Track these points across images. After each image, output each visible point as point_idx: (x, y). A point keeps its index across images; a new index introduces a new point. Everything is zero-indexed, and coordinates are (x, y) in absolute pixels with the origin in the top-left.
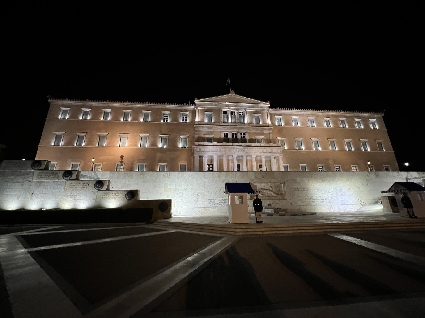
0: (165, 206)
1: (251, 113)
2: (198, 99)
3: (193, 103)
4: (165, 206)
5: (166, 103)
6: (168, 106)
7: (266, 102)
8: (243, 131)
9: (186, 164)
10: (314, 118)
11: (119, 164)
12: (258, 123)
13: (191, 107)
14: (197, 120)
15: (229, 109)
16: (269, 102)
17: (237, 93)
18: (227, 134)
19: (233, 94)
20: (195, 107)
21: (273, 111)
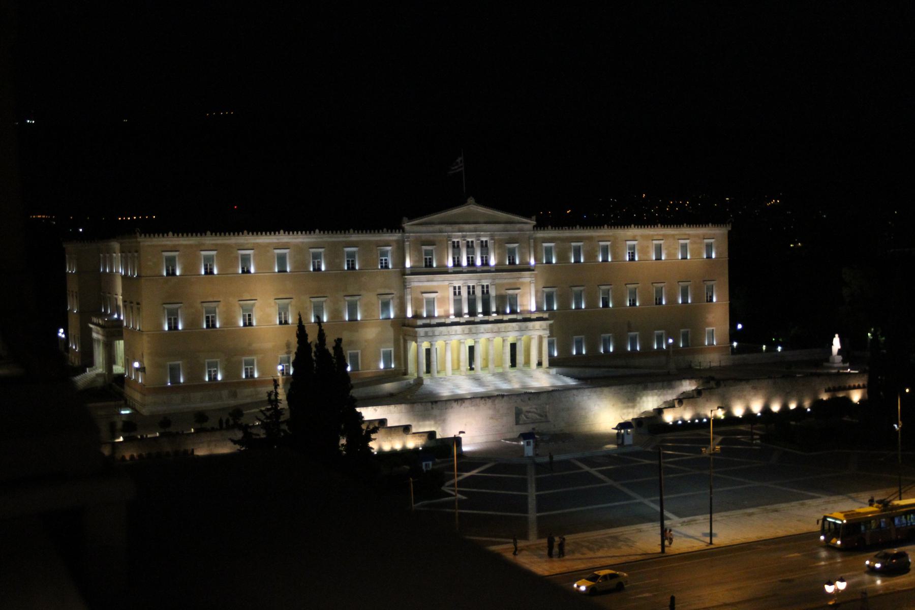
0: (457, 441)
1: (500, 244)
2: (411, 218)
3: (400, 229)
4: (457, 441)
5: (351, 231)
6: (355, 237)
7: (528, 216)
8: (485, 283)
9: (392, 349)
10: (609, 243)
11: (285, 356)
12: (512, 262)
13: (395, 237)
14: (408, 264)
15: (464, 237)
16: (534, 218)
17: (480, 202)
18: (459, 288)
19: (473, 208)
20: (403, 237)
21: (540, 234)
